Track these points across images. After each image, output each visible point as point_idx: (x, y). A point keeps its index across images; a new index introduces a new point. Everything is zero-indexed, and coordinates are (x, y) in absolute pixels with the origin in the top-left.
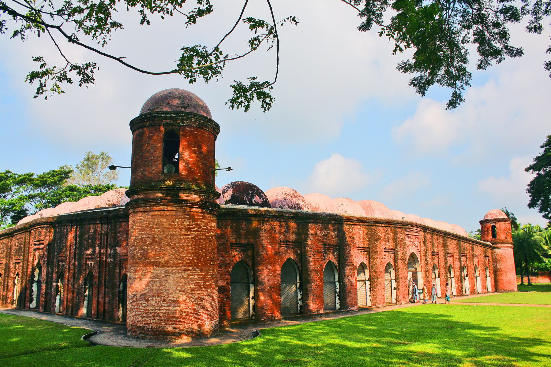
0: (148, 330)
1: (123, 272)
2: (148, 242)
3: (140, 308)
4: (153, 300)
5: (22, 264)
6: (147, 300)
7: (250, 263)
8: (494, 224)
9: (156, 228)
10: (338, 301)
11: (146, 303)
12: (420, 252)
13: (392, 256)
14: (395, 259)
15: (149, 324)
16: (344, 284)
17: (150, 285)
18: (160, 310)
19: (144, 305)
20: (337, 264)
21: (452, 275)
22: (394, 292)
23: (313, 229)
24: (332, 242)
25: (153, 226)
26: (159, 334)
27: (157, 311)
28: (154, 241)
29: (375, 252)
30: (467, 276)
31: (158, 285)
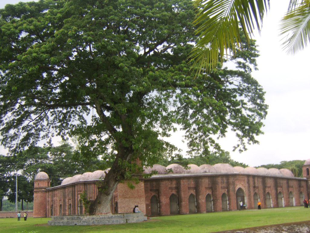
1: (116, 200)
7: (157, 196)
8: (308, 168)
10: (196, 209)
12: (245, 187)
13: (226, 190)
14: (228, 191)
16: (198, 203)
20: (195, 194)
21: (271, 197)
22: (228, 206)
23: (182, 182)
24: (192, 186)
28: (125, 191)
29: (216, 189)
30: (283, 197)
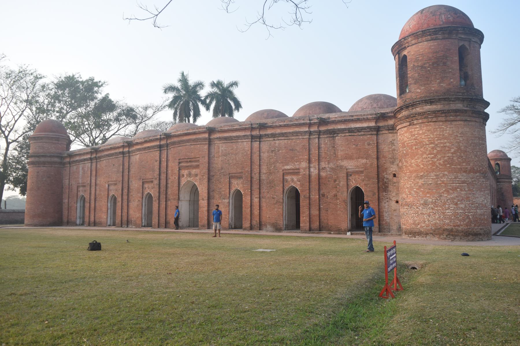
0: (457, 231)
2: (453, 150)
3: (447, 211)
4: (462, 203)
5: (156, 182)
6: (456, 204)
9: (461, 137)
11: (455, 206)
15: (458, 226)
17: (458, 190)
18: (469, 212)
19: (452, 208)
25: (457, 135)
26: (469, 236)
27: (466, 213)
31: (466, 189)
